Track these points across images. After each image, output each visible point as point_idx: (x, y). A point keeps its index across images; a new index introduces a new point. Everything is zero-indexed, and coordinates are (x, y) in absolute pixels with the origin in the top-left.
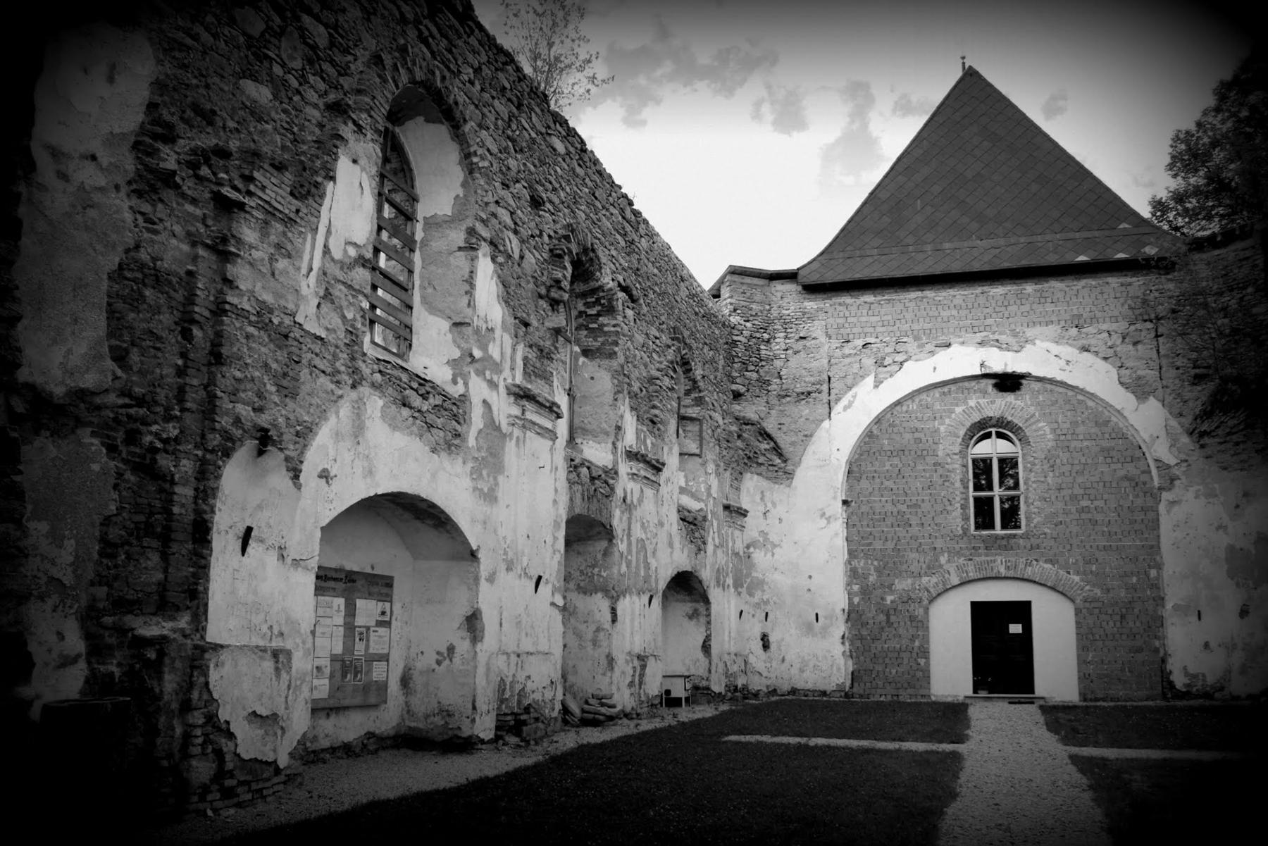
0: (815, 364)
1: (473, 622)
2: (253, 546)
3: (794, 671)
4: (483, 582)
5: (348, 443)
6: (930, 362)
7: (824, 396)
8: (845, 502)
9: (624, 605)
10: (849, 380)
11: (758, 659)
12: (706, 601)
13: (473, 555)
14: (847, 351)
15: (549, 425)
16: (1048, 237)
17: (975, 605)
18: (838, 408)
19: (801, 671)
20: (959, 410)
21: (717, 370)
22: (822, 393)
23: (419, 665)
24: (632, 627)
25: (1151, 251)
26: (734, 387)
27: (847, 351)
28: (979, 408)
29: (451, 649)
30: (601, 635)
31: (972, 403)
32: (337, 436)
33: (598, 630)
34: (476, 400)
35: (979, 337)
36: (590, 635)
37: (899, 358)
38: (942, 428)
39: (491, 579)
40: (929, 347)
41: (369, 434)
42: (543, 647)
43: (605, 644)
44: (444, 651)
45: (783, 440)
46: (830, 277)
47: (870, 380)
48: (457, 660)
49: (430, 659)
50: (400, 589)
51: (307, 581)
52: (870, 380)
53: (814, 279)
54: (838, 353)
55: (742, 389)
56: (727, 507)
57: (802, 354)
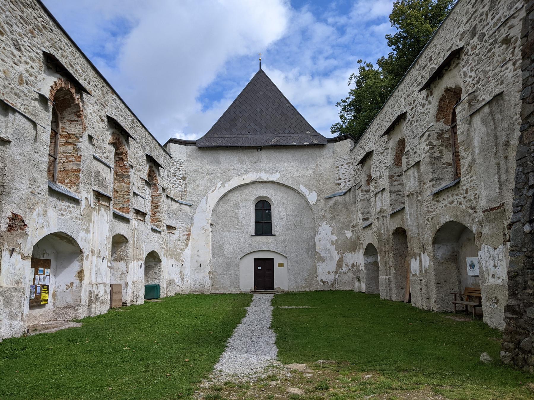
1: (80, 274)
2: (14, 253)
3: (192, 285)
4: (84, 260)
5: (42, 217)
8: (211, 225)
9: (131, 265)
11: (178, 282)
12: (160, 261)
13: (81, 252)
15: (108, 205)
16: (283, 135)
17: (254, 259)
19: (194, 284)
23: (59, 290)
24: (134, 272)
25: (316, 142)
29: (72, 284)
30: (123, 276)
32: (39, 215)
33: (122, 274)
34: (83, 198)
36: (119, 276)
39: (87, 259)
41: (48, 213)
42: (104, 281)
43: (124, 278)
44: (69, 284)
46: (207, 144)
48: (74, 287)
49: (64, 287)
50: (53, 264)
51: (28, 262)
53: (202, 144)
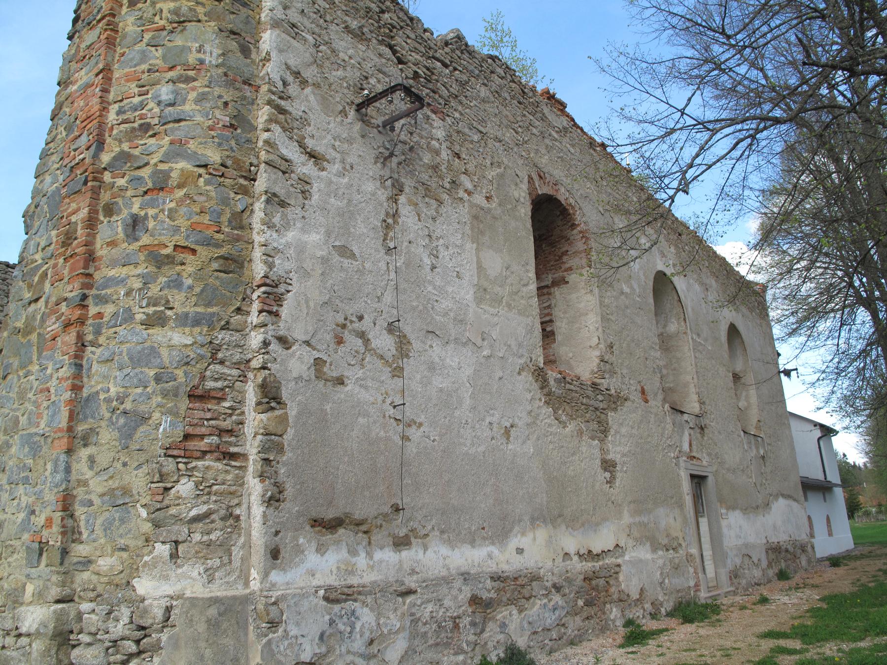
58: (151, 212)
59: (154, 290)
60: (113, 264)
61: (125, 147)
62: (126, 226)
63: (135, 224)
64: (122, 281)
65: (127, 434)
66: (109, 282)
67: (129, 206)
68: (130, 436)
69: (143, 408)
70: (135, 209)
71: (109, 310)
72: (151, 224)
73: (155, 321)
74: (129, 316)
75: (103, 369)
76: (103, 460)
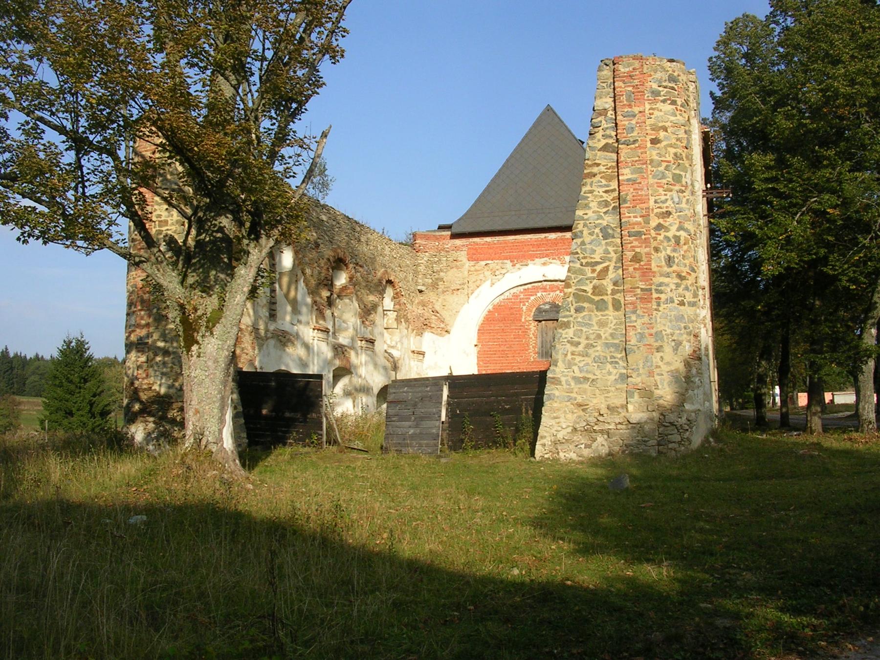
0: (460, 275)
6: (519, 273)
7: (466, 292)
10: (478, 283)
14: (477, 267)
18: (472, 297)
20: (532, 298)
21: (408, 281)
22: (463, 289)
26: (419, 288)
27: (477, 267)
28: (542, 298)
31: (539, 295)
35: (543, 260)
37: (504, 271)
38: (524, 308)
40: (518, 266)
45: (445, 314)
47: (488, 283)
52: (488, 283)
54: (473, 269)
55: (423, 288)
56: (413, 352)
57: (455, 269)
58: (676, 255)
59: (680, 290)
60: (661, 275)
61: (661, 221)
62: (665, 259)
63: (669, 260)
64: (667, 285)
65: (676, 349)
66: (661, 284)
67: (665, 250)
68: (677, 350)
69: (680, 339)
70: (669, 252)
71: (663, 296)
72: (676, 260)
73: (682, 303)
74: (672, 301)
75: (663, 321)
76: (667, 358)
